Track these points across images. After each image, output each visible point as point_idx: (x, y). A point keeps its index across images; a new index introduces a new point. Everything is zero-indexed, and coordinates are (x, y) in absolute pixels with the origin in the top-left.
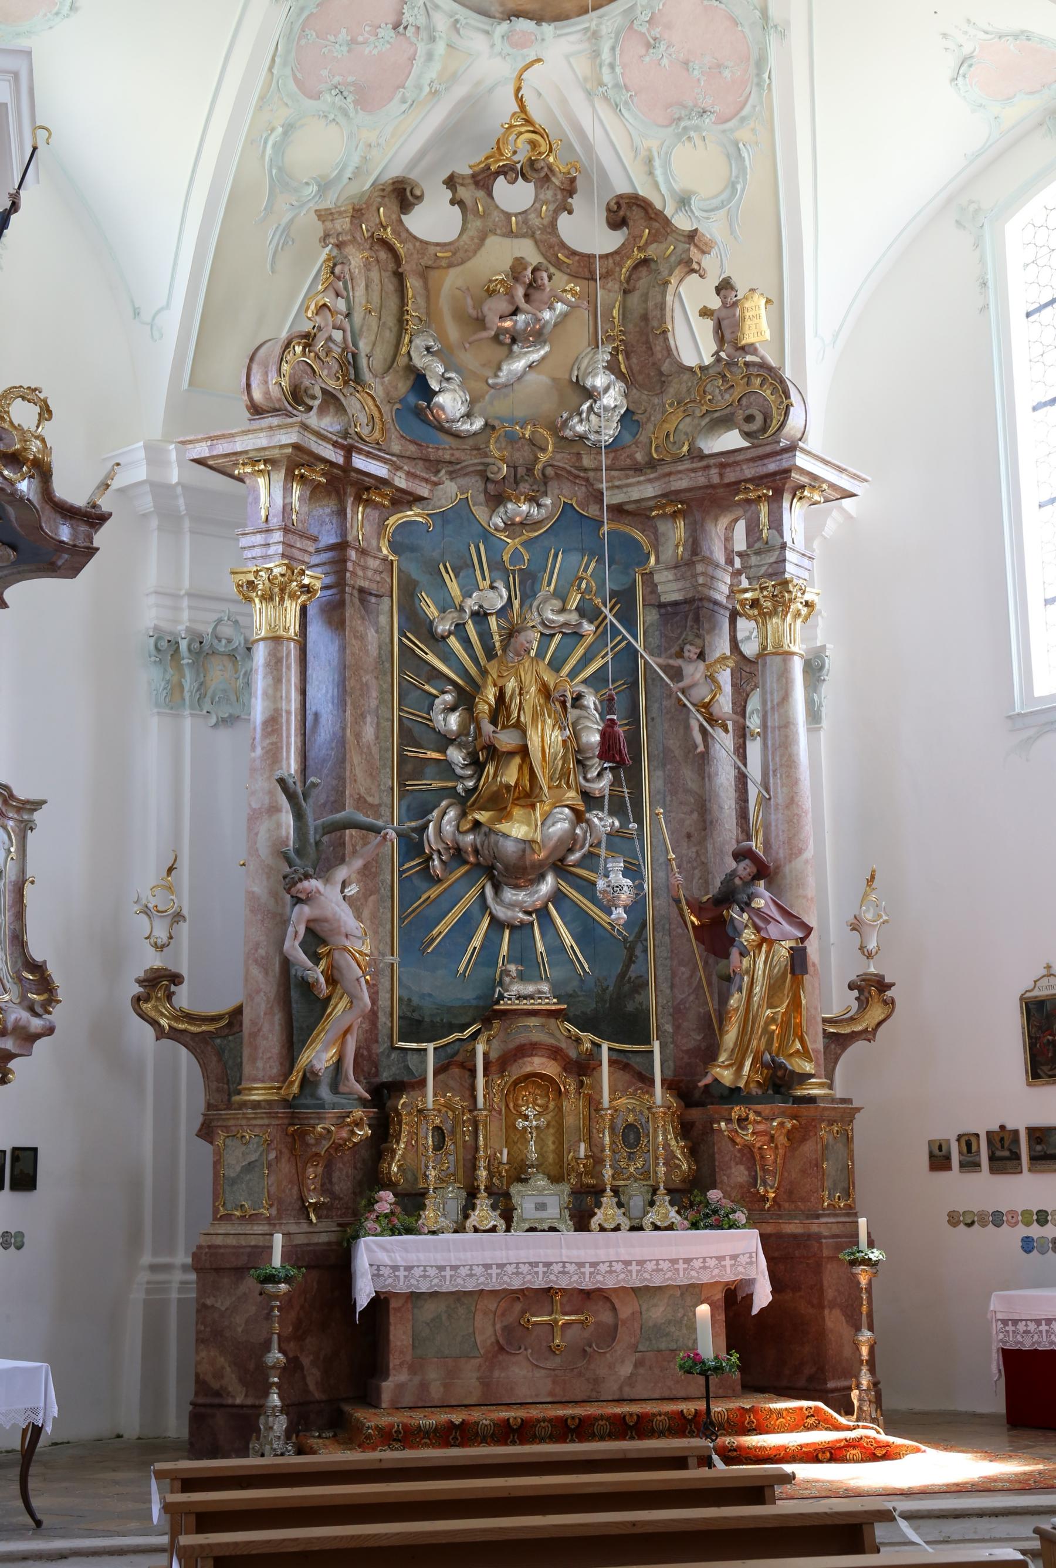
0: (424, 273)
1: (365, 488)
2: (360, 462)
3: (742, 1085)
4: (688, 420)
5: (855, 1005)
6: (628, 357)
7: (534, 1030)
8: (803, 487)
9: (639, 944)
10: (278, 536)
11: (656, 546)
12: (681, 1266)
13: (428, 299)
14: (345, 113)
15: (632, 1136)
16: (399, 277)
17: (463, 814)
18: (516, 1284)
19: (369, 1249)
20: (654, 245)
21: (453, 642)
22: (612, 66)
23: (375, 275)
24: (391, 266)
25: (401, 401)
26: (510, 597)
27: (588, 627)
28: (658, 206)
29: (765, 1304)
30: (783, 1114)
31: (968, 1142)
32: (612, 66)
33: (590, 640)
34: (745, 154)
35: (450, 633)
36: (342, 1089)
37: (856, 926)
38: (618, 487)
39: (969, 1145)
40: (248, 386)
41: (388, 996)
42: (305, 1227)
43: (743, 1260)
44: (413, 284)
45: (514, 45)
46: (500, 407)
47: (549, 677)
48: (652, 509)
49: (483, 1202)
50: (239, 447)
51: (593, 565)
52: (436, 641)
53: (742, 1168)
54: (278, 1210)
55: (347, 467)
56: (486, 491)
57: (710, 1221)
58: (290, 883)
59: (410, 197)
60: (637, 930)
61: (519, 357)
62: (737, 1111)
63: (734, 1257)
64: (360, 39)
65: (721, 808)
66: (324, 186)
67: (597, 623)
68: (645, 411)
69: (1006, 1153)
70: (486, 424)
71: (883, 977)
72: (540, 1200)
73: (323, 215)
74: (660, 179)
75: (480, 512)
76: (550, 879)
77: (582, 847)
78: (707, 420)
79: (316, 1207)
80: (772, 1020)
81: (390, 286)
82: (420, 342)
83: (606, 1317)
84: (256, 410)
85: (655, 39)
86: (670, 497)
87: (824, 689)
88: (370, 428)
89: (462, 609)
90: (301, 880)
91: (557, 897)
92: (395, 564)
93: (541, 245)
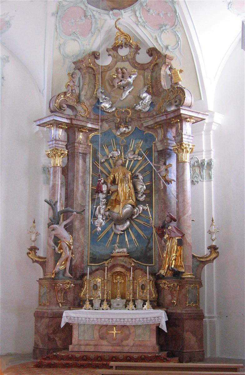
2: (74, 122)
4: (165, 103)
5: (209, 253)
6: (152, 88)
7: (121, 261)
8: (187, 118)
9: (151, 239)
11: (157, 136)
15: (143, 287)
16: (94, 75)
20: (158, 60)
22: (141, 17)
23: (87, 76)
24: (93, 73)
26: (121, 153)
27: (140, 158)
30: (176, 281)
32: (141, 17)
33: (141, 161)
34: (179, 35)
35: (104, 162)
36: (66, 275)
37: (210, 232)
38: (146, 122)
41: (87, 252)
44: (99, 77)
45: (115, 16)
46: (119, 104)
47: (126, 171)
48: (155, 127)
49: (105, 303)
53: (170, 296)
54: (49, 304)
55: (71, 123)
56: (115, 126)
58: (49, 225)
59: (96, 56)
60: (151, 235)
62: (164, 281)
64: (77, 21)
65: (170, 203)
67: (143, 157)
68: (156, 102)
70: (116, 109)
74: (160, 43)
75: (114, 131)
76: (128, 223)
77: (136, 214)
78: (168, 103)
82: (100, 90)
83: (127, 332)
85: (149, 9)
87: (213, 170)
88: (85, 113)
89: (108, 156)
90: (51, 225)
91: (131, 226)
92: (91, 146)
93: (131, 63)
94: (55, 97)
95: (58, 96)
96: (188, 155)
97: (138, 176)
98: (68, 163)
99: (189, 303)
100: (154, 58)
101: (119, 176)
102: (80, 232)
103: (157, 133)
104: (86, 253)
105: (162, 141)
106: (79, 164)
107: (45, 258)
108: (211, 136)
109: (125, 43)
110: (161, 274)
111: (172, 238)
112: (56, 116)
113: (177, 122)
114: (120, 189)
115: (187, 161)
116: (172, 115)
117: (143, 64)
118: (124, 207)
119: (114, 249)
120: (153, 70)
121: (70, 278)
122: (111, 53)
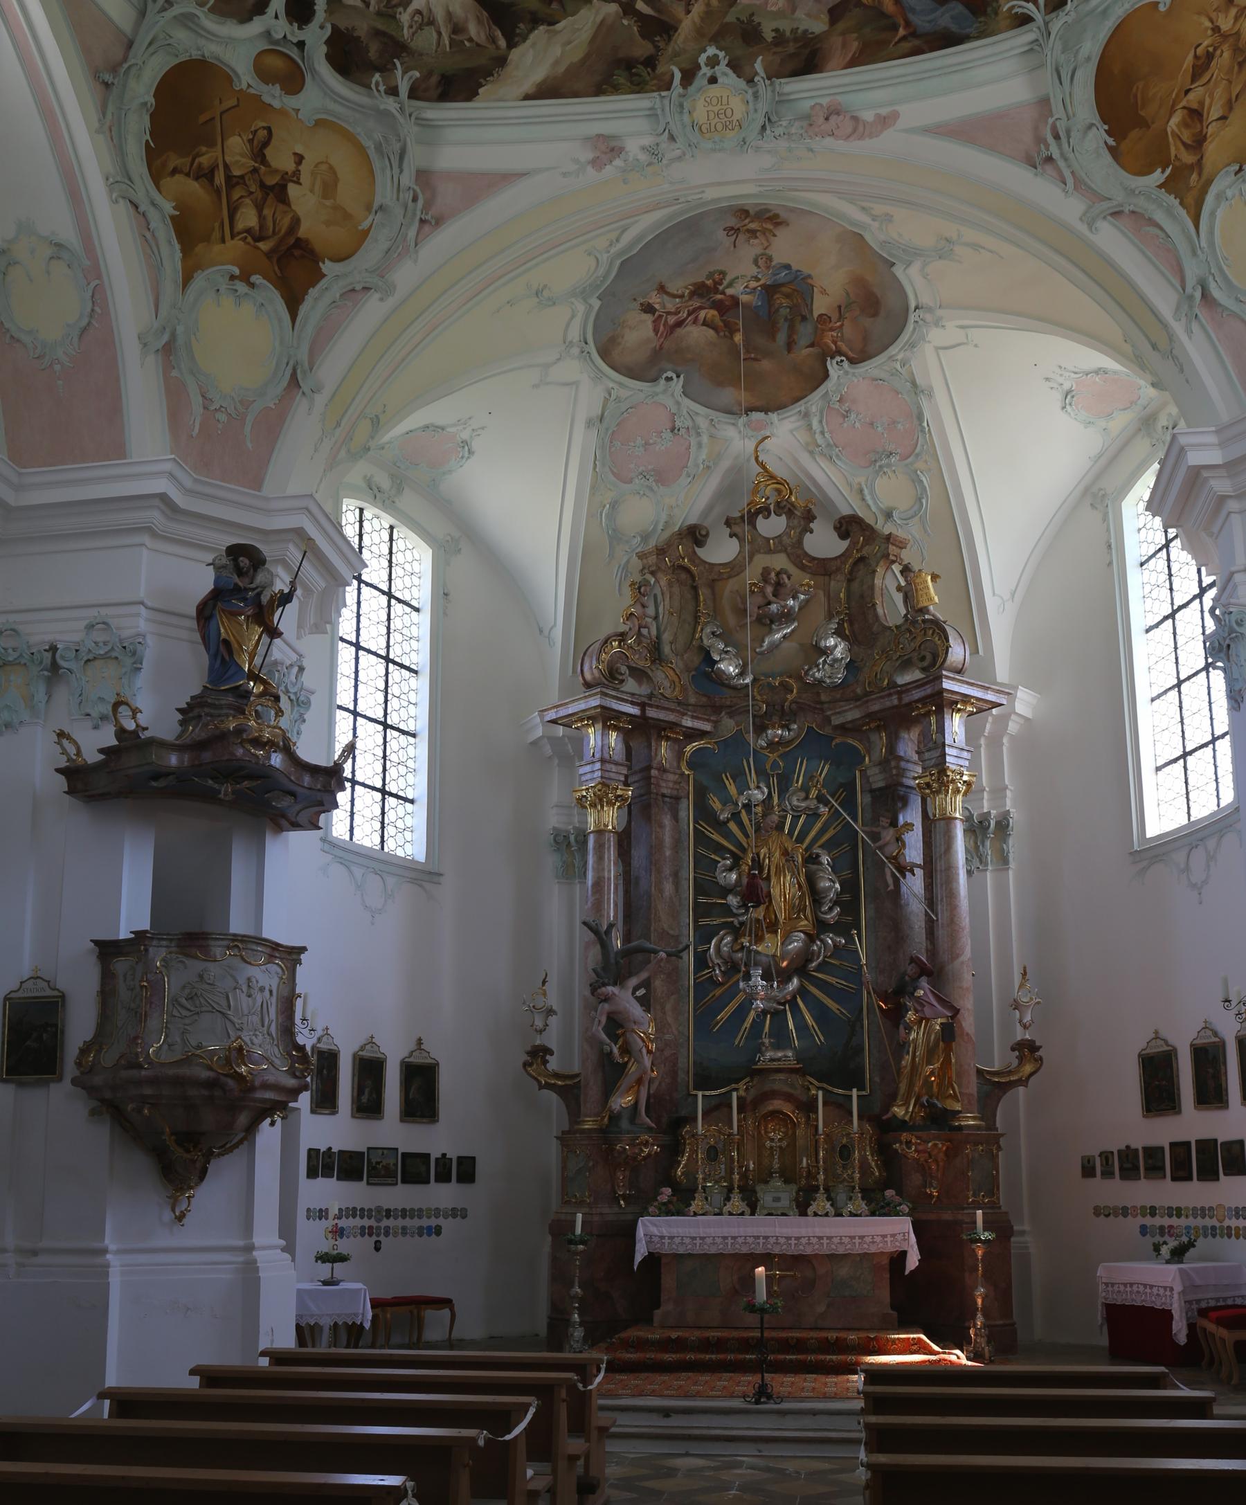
0: (712, 584)
1: (661, 730)
2: (651, 713)
3: (907, 1118)
5: (1016, 1062)
6: (851, 623)
7: (778, 1082)
10: (598, 766)
12: (857, 1241)
13: (714, 600)
14: (652, 490)
17: (735, 940)
18: (745, 1250)
19: (644, 1225)
21: (732, 826)
23: (676, 589)
24: (690, 582)
25: (696, 669)
26: (770, 793)
27: (823, 809)
28: (872, 523)
29: (913, 1268)
31: (1106, 1156)
35: (728, 820)
39: (1107, 1158)
40: (582, 671)
42: (616, 1209)
43: (899, 1237)
44: (703, 593)
50: (570, 711)
51: (827, 767)
52: (720, 826)
55: (643, 715)
57: (885, 1211)
58: (594, 989)
61: (778, 631)
62: (905, 1136)
63: (893, 1236)
65: (911, 928)
66: (645, 537)
69: (1129, 1166)
71: (1034, 1042)
72: (776, 1195)
73: (641, 556)
76: (795, 981)
79: (624, 1197)
80: (932, 1074)
81: (689, 596)
82: (708, 630)
84: (588, 685)
86: (870, 716)
87: (1011, 841)
91: (802, 991)
94: (597, 645)
95: (606, 642)
96: (959, 798)
97: (818, 856)
98: (629, 822)
99: (974, 1195)
100: (853, 544)
101: (771, 854)
102: (668, 1007)
103: (869, 742)
104: (682, 1062)
105: (884, 763)
106: (661, 826)
107: (577, 1075)
108: (1005, 749)
109: (778, 504)
110: (894, 1116)
111: (928, 1020)
112: (606, 695)
113: (928, 714)
114: (775, 892)
115: (957, 815)
116: (917, 694)
117: (824, 559)
118: (787, 939)
119: (759, 1050)
120: (851, 573)
121: (650, 1129)
122: (737, 529)
